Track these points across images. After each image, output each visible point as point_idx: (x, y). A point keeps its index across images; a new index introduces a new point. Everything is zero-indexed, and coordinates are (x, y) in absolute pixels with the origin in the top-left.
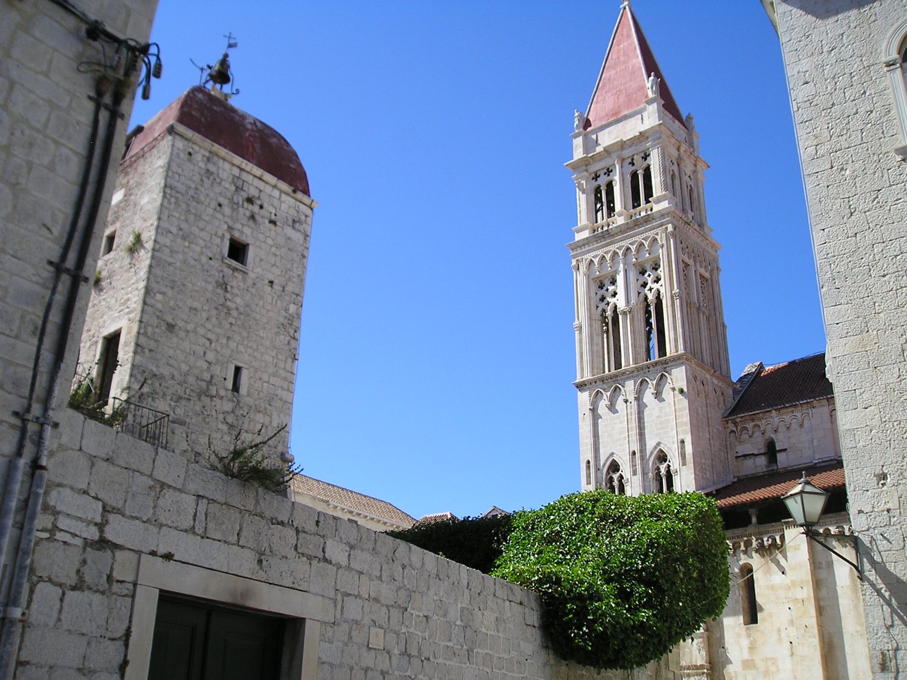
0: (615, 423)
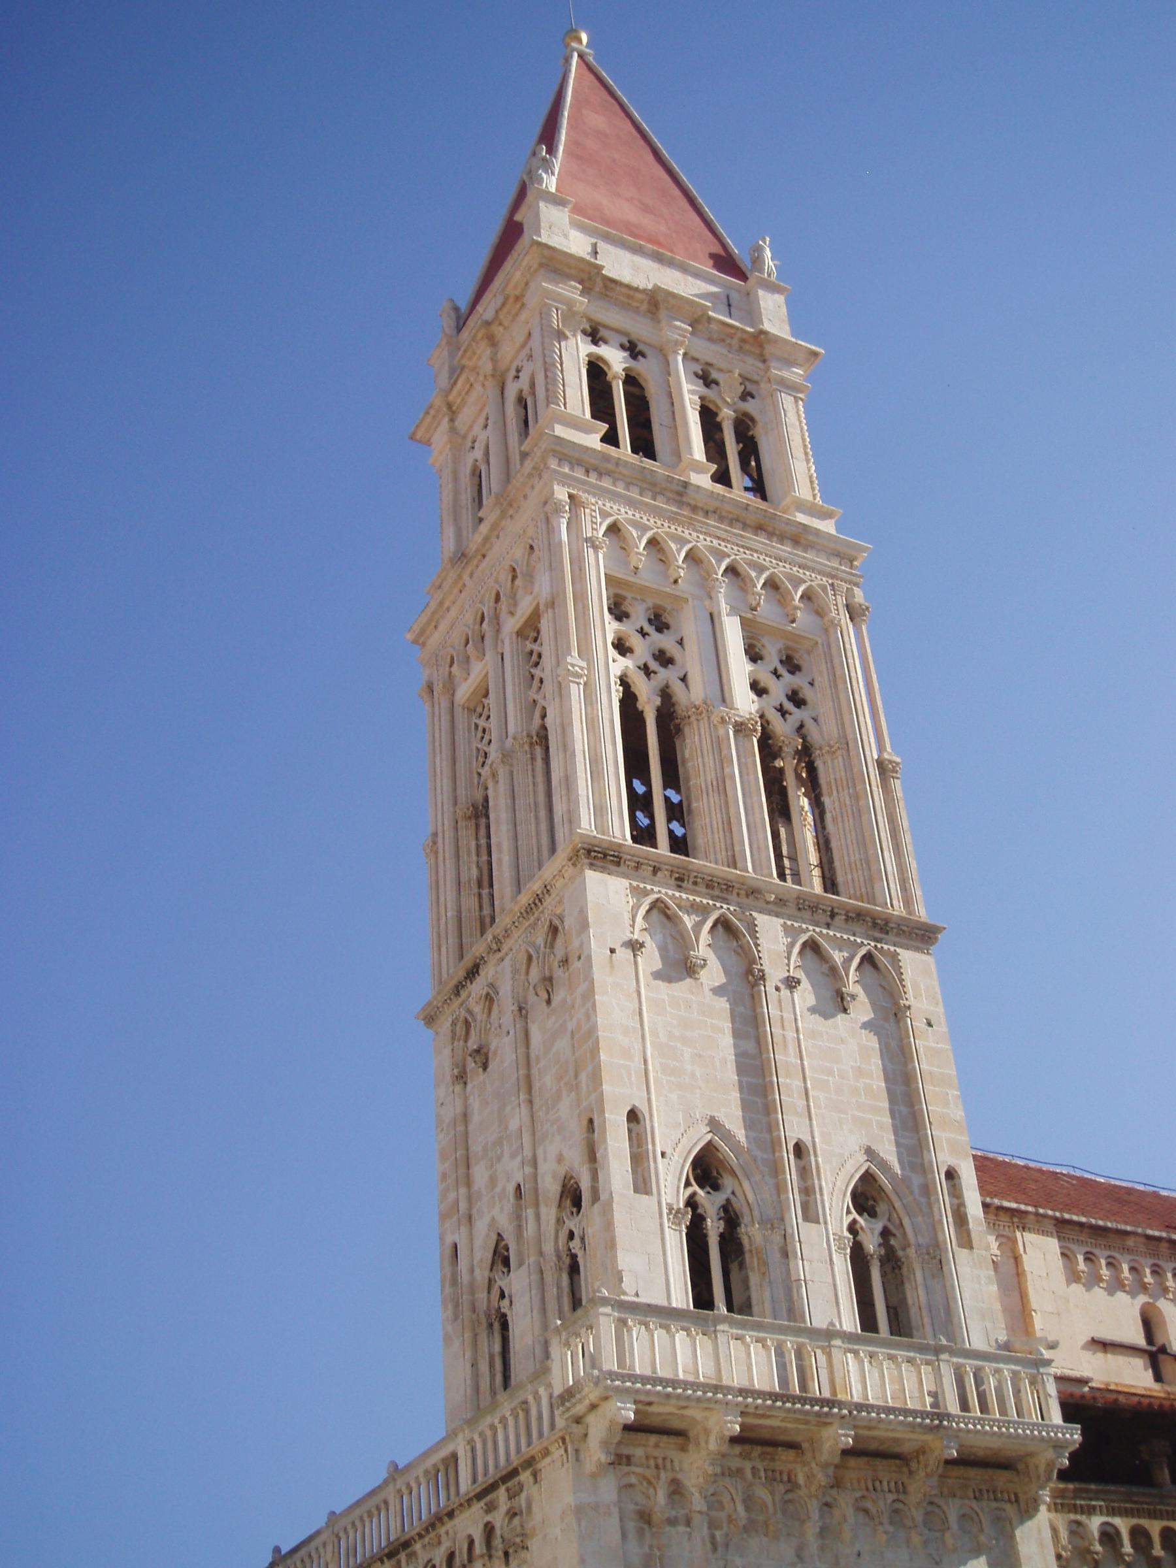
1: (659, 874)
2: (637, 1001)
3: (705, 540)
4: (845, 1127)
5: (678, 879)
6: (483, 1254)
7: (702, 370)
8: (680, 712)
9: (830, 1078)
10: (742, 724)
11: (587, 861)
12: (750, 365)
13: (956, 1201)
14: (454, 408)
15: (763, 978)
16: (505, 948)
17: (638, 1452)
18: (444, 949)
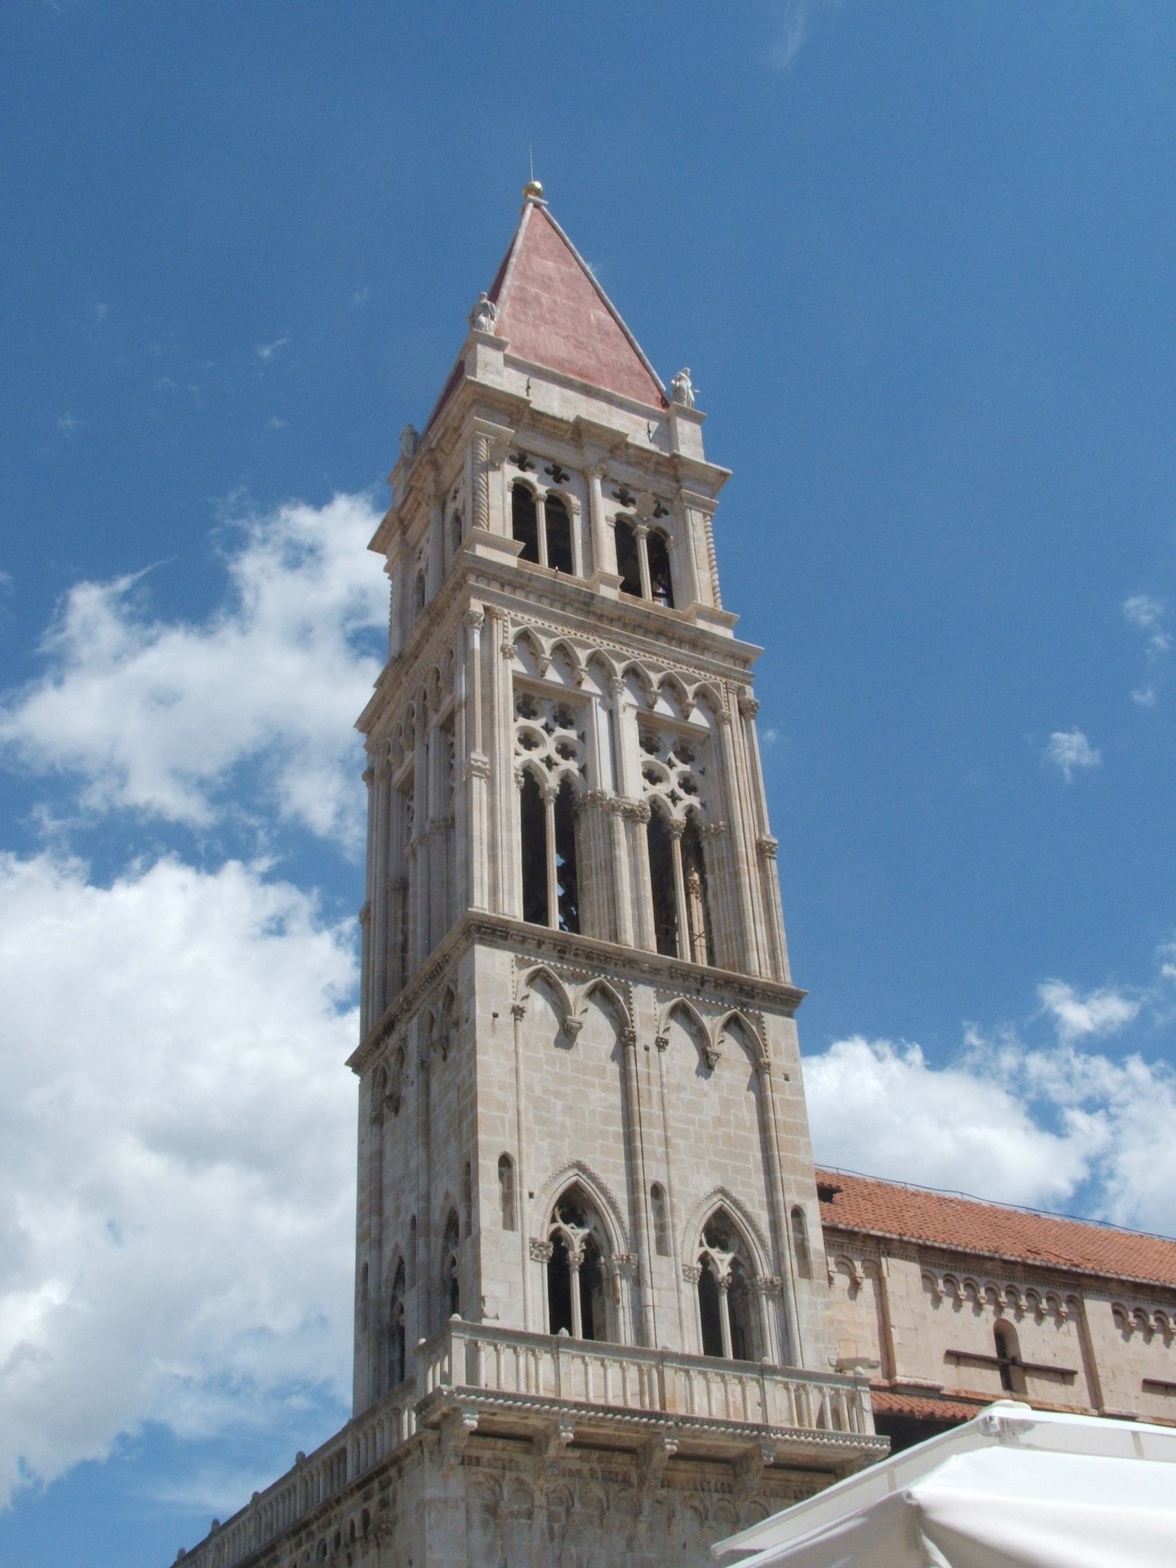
0: (592, 1085)
1: (544, 947)
2: (514, 1059)
3: (608, 645)
4: (702, 1171)
5: (559, 951)
6: (388, 1273)
7: (620, 490)
8: (577, 800)
9: (691, 1128)
10: (631, 811)
11: (477, 936)
12: (663, 486)
13: (800, 1236)
14: (405, 523)
15: (633, 1039)
16: (414, 1008)
17: (487, 1455)
18: (370, 1006)
